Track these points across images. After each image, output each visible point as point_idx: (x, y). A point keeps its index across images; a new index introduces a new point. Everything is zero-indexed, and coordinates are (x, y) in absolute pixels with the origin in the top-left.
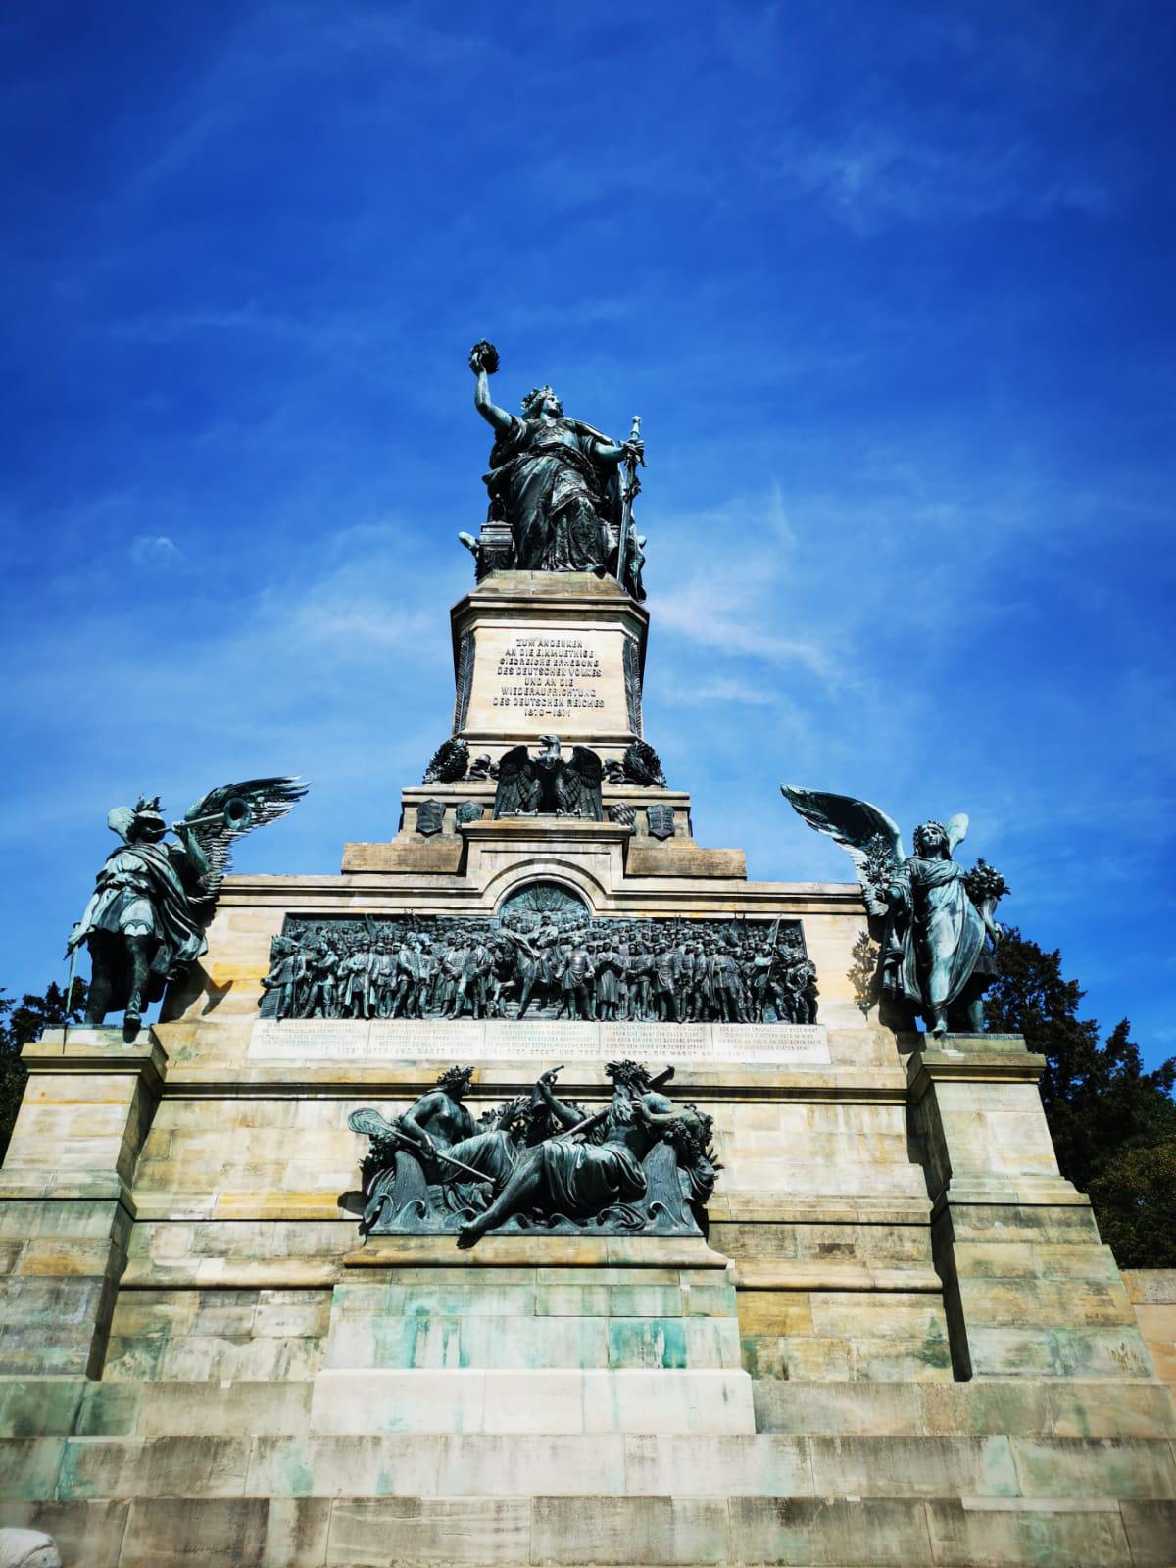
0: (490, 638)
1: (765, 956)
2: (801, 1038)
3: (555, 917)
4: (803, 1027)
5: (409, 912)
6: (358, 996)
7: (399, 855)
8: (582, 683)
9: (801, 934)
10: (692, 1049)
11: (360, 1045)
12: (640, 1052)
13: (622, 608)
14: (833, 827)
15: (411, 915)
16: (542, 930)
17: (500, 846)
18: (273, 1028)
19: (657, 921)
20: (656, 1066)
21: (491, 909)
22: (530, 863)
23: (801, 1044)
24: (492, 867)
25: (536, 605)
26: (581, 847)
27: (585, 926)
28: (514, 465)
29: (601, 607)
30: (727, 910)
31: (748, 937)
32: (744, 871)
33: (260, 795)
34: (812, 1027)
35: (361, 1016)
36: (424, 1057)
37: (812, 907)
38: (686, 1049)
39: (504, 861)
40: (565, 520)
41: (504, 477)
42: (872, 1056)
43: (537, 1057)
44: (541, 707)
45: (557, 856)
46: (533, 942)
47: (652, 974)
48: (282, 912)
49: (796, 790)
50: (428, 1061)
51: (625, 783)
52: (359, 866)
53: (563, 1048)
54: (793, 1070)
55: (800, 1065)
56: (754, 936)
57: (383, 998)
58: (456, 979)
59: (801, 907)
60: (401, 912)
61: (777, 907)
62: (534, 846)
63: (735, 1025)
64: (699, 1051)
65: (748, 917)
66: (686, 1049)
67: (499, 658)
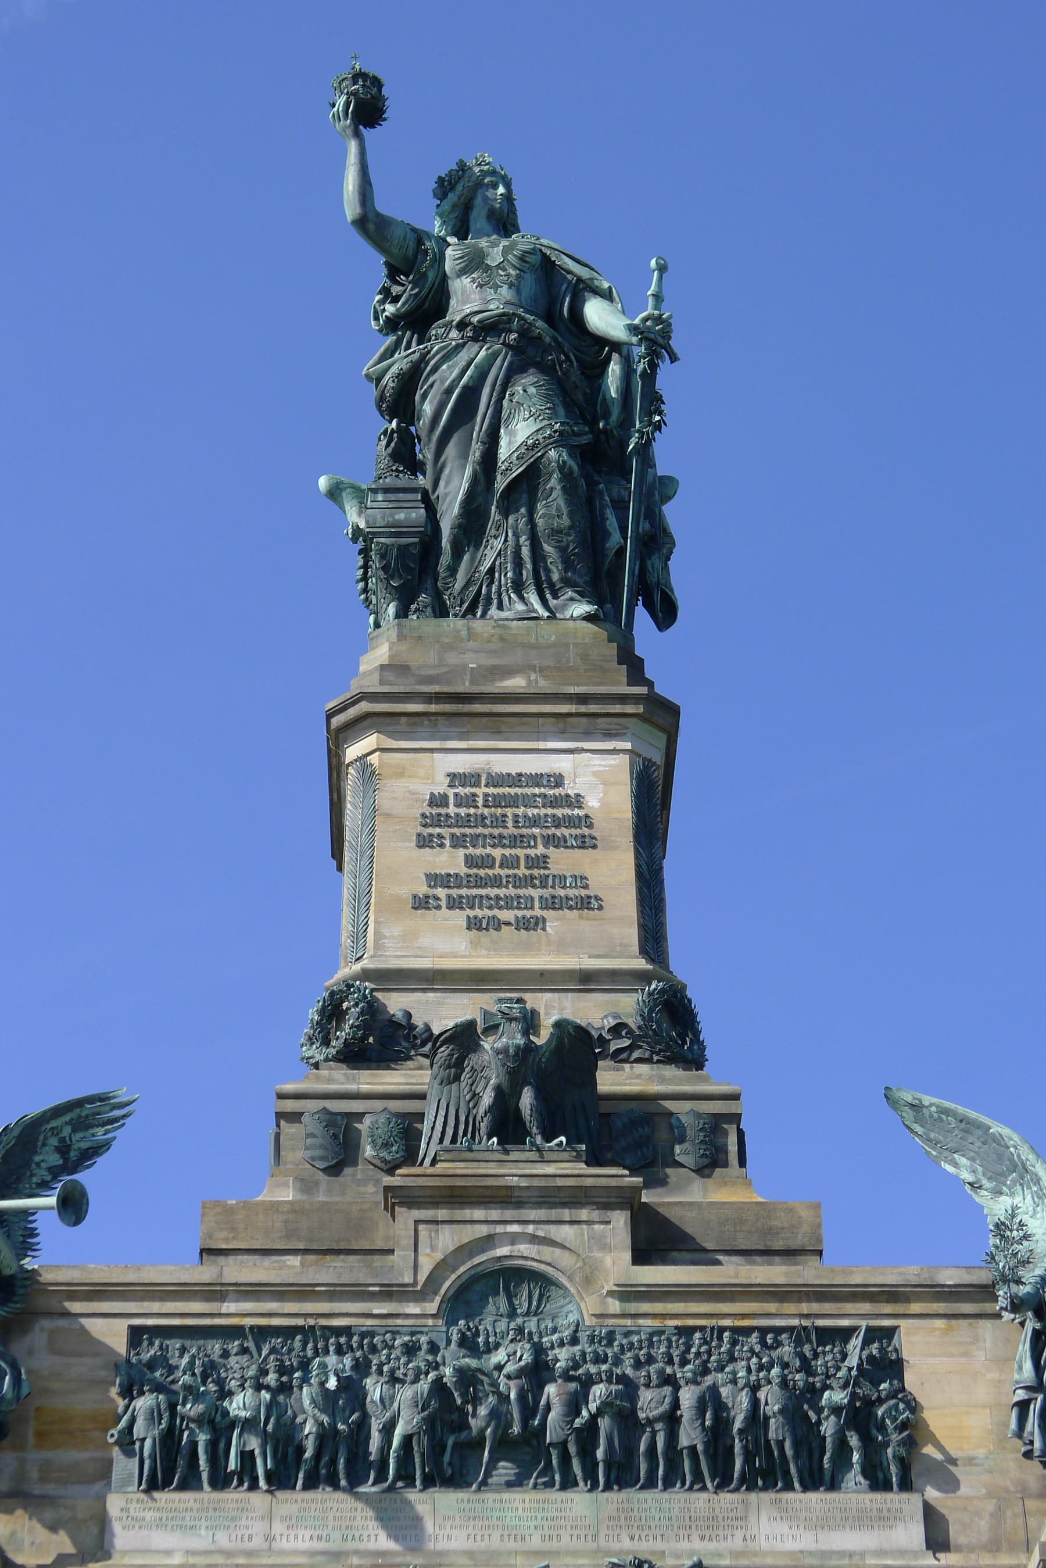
0: (400, 773)
1: (845, 1386)
2: (885, 1513)
3: (531, 1325)
4: (889, 1496)
5: (311, 1322)
6: (247, 1457)
7: (285, 1222)
8: (562, 861)
9: (896, 1350)
10: (730, 1532)
11: (258, 1528)
12: (655, 1538)
13: (630, 709)
14: (963, 1161)
15: (313, 1327)
16: (510, 1349)
17: (442, 1214)
18: (134, 1504)
19: (681, 1331)
20: (678, 1556)
21: (433, 1316)
22: (488, 1241)
23: (884, 1520)
24: (433, 1248)
25: (478, 708)
26: (566, 1214)
27: (574, 1341)
28: (423, 359)
29: (593, 708)
30: (788, 1315)
31: (816, 1356)
32: (819, 1241)
33: (67, 1123)
34: (905, 1496)
35: (254, 1486)
36: (350, 1546)
37: (916, 1308)
38: (720, 1532)
39: (447, 1239)
40: (525, 497)
41: (410, 381)
42: (985, 1538)
43: (511, 1545)
44: (496, 912)
45: (530, 1229)
46: (499, 1368)
47: (672, 1419)
48: (121, 1326)
49: (908, 1097)
50: (356, 1552)
51: (639, 1060)
52: (226, 1240)
53: (547, 1532)
54: (871, 1561)
55: (881, 1553)
56: (824, 1353)
57: (285, 1455)
58: (388, 1429)
59: (899, 1308)
60: (300, 1322)
61: (865, 1307)
62: (495, 1214)
63: (790, 1496)
64: (739, 1534)
65: (821, 1323)
66: (720, 1532)
67: (417, 812)
